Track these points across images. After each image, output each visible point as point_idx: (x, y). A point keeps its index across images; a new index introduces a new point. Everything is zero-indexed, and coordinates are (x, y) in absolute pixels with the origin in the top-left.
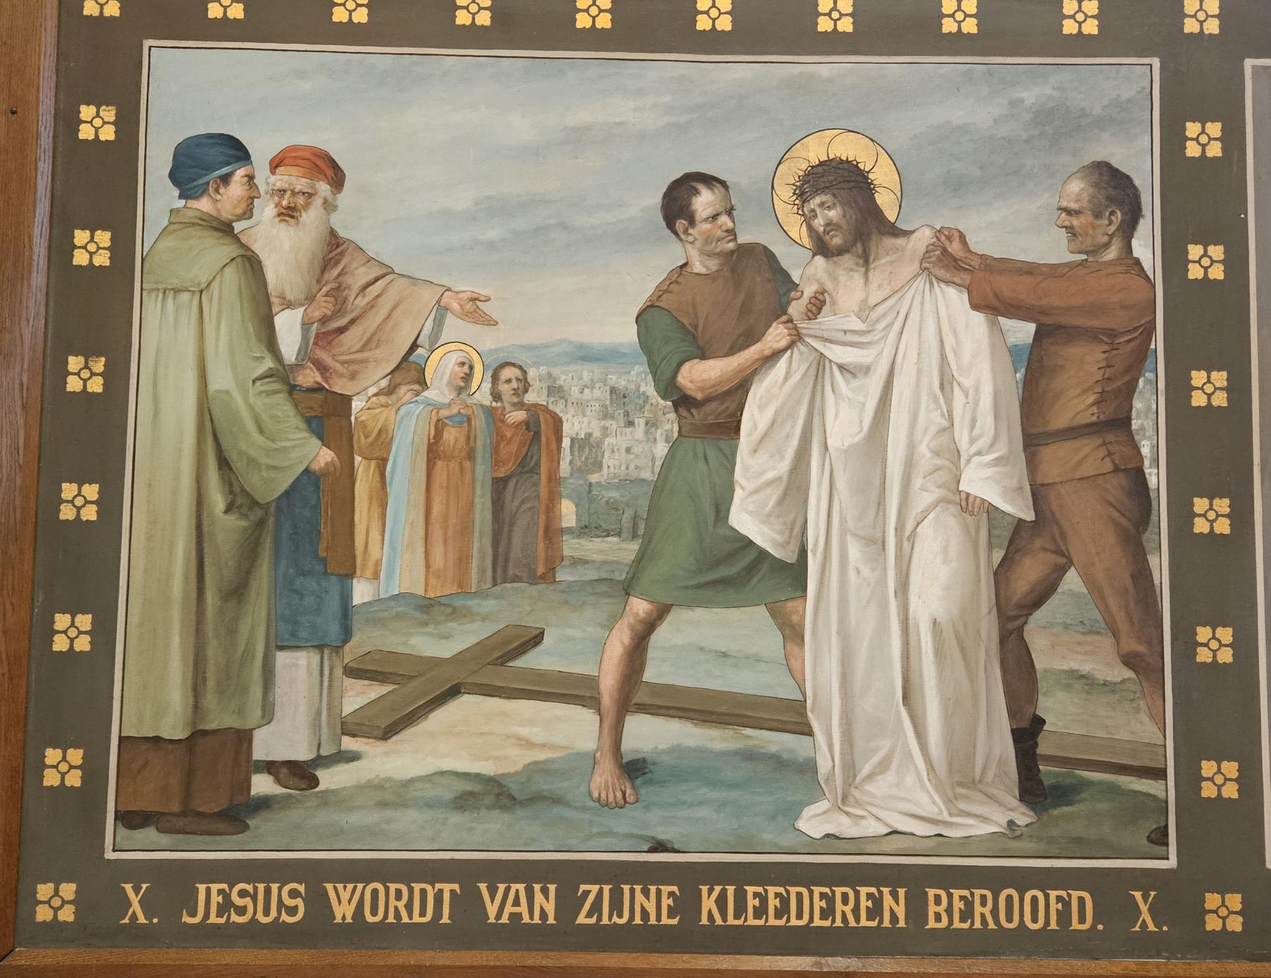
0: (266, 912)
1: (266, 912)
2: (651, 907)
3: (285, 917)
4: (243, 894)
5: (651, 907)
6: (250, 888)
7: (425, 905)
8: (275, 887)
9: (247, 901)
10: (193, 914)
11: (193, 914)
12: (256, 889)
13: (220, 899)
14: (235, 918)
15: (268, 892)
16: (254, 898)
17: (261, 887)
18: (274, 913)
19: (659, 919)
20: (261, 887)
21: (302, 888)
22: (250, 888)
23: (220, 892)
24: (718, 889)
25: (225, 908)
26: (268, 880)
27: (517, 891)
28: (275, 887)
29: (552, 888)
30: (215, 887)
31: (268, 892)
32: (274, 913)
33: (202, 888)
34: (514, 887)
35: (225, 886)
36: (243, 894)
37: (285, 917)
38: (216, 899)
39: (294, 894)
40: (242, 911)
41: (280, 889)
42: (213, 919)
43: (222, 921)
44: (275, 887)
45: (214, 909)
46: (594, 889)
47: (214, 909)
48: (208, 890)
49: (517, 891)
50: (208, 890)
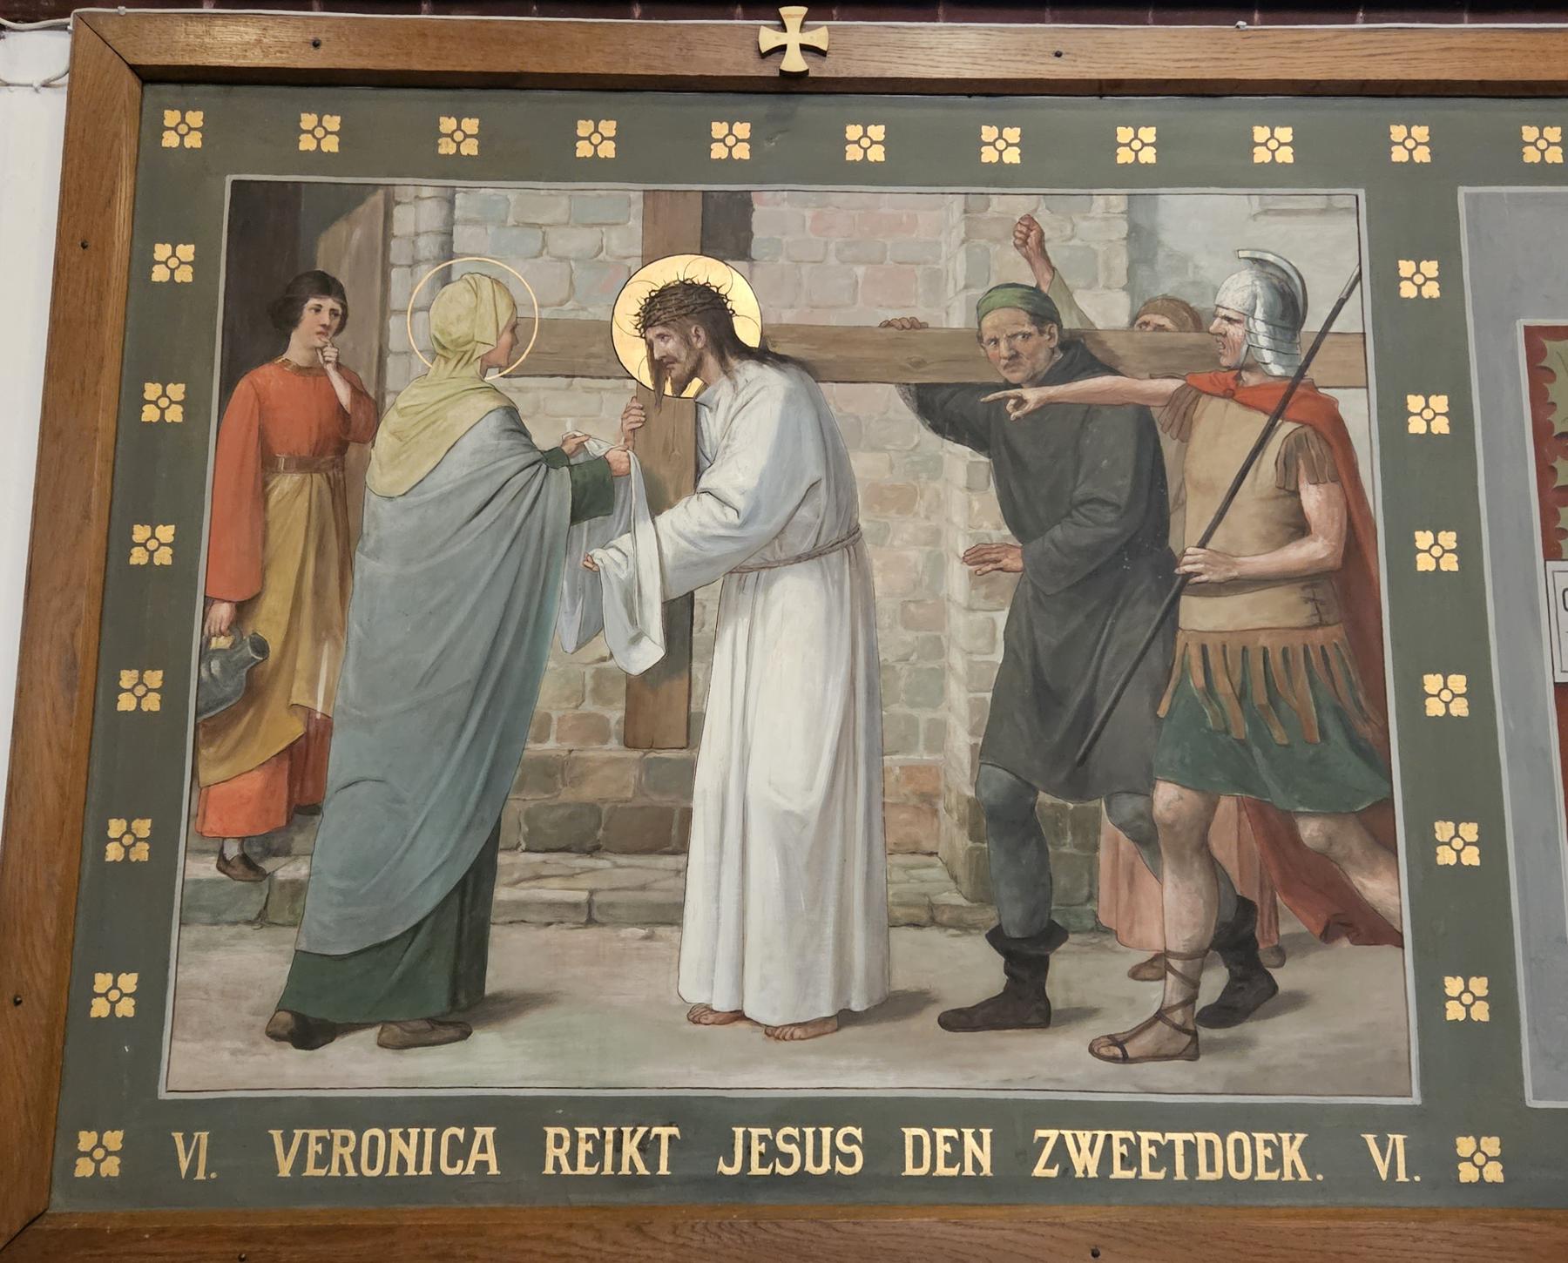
0: (818, 1161)
1: (818, 1161)
4: (788, 1139)
6: (795, 1132)
7: (836, 1152)
8: (826, 1132)
9: (793, 1149)
12: (803, 1135)
15: (818, 1136)
16: (802, 1146)
17: (809, 1131)
20: (809, 1131)
22: (795, 1132)
24: (642, 1130)
26: (818, 1123)
27: (484, 1138)
29: (986, 1132)
30: (755, 1132)
31: (818, 1136)
34: (480, 1131)
35: (767, 1131)
36: (788, 1139)
38: (757, 1148)
39: (849, 1139)
40: (787, 1160)
45: (755, 1158)
46: (1053, 1134)
47: (755, 1158)
48: (747, 1136)
49: (484, 1138)
50: (747, 1136)
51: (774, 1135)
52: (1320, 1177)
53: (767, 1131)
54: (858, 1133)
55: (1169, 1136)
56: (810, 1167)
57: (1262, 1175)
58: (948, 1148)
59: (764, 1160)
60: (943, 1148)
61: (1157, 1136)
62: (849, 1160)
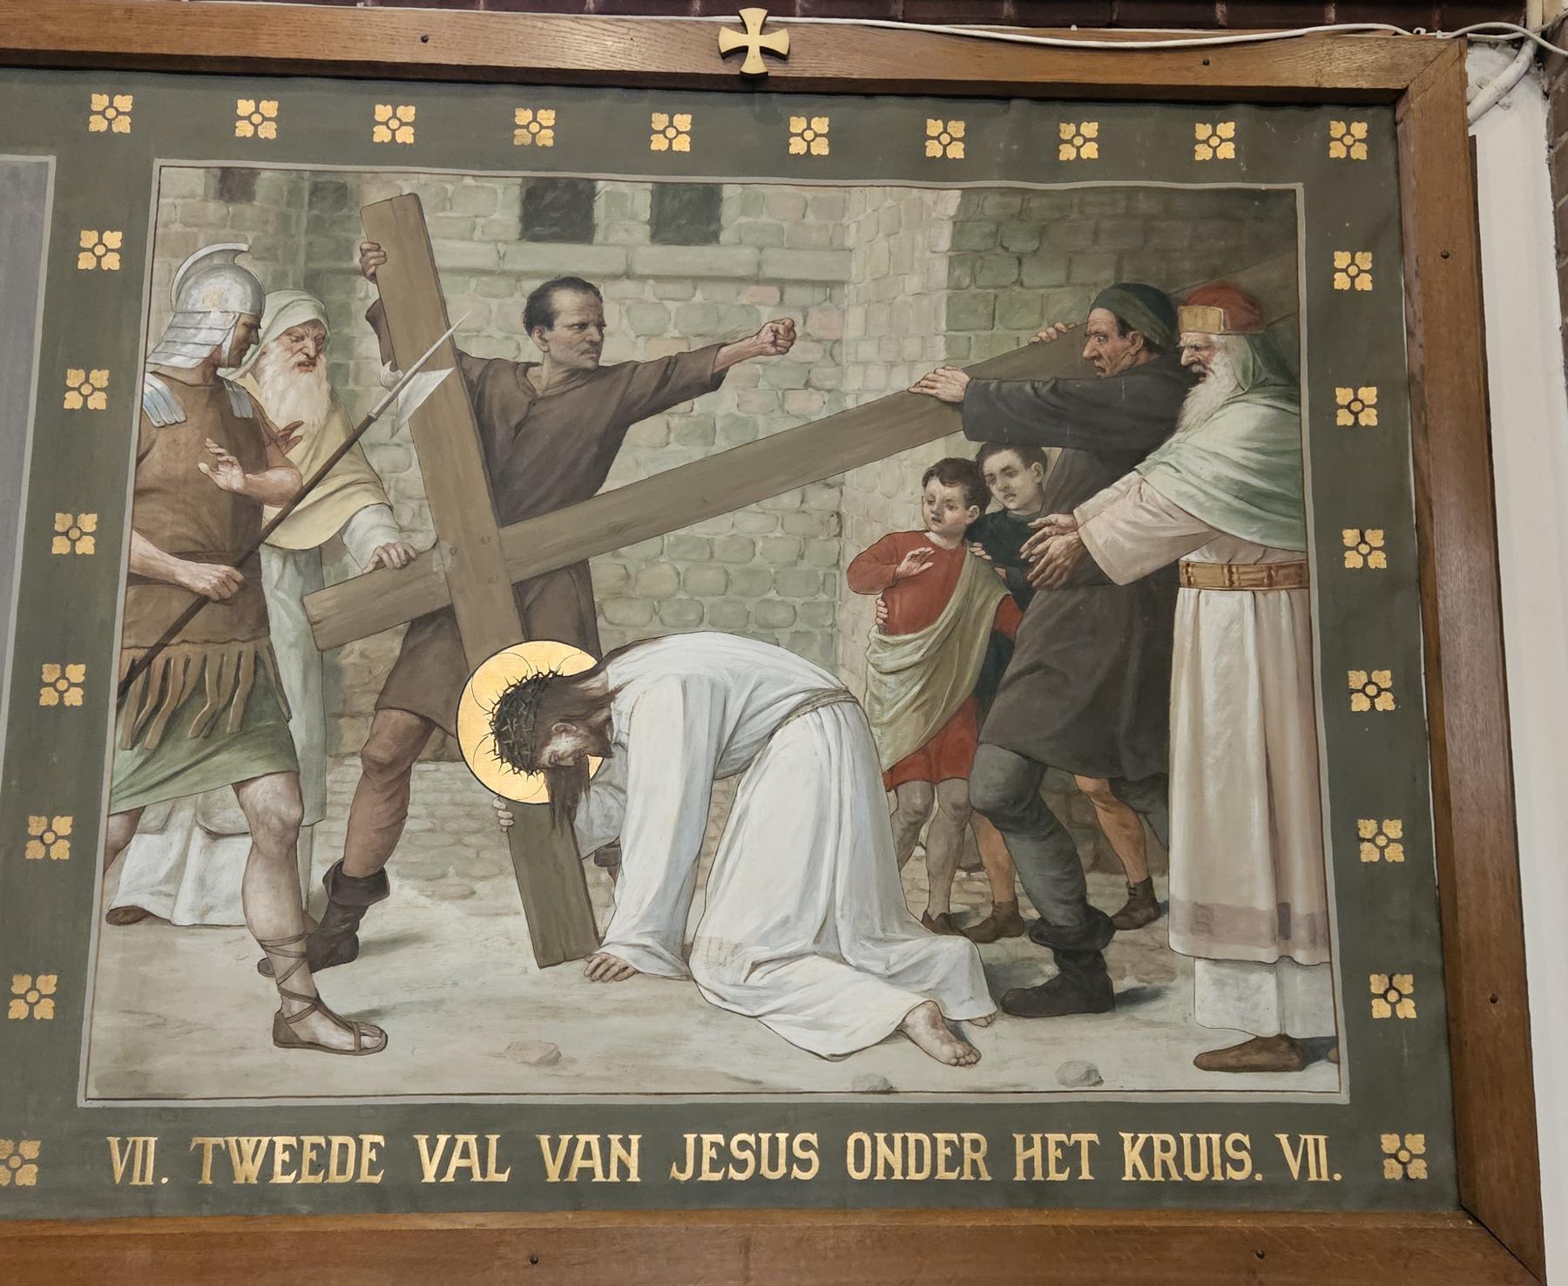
1: (773, 1166)
4: (743, 1145)
6: (751, 1139)
9: (748, 1155)
11: (682, 1170)
12: (758, 1141)
14: (734, 1174)
15: (774, 1142)
17: (765, 1137)
20: (765, 1137)
22: (751, 1139)
25: (723, 1157)
26: (773, 1128)
30: (707, 1139)
31: (774, 1142)
33: (690, 1138)
36: (743, 1145)
38: (709, 1153)
40: (741, 1165)
41: (790, 1141)
42: (707, 1175)
43: (718, 1176)
44: (782, 1137)
47: (706, 1166)
48: (699, 1143)
50: (699, 1143)
51: (728, 1140)
54: (813, 1138)
62: (805, 1165)
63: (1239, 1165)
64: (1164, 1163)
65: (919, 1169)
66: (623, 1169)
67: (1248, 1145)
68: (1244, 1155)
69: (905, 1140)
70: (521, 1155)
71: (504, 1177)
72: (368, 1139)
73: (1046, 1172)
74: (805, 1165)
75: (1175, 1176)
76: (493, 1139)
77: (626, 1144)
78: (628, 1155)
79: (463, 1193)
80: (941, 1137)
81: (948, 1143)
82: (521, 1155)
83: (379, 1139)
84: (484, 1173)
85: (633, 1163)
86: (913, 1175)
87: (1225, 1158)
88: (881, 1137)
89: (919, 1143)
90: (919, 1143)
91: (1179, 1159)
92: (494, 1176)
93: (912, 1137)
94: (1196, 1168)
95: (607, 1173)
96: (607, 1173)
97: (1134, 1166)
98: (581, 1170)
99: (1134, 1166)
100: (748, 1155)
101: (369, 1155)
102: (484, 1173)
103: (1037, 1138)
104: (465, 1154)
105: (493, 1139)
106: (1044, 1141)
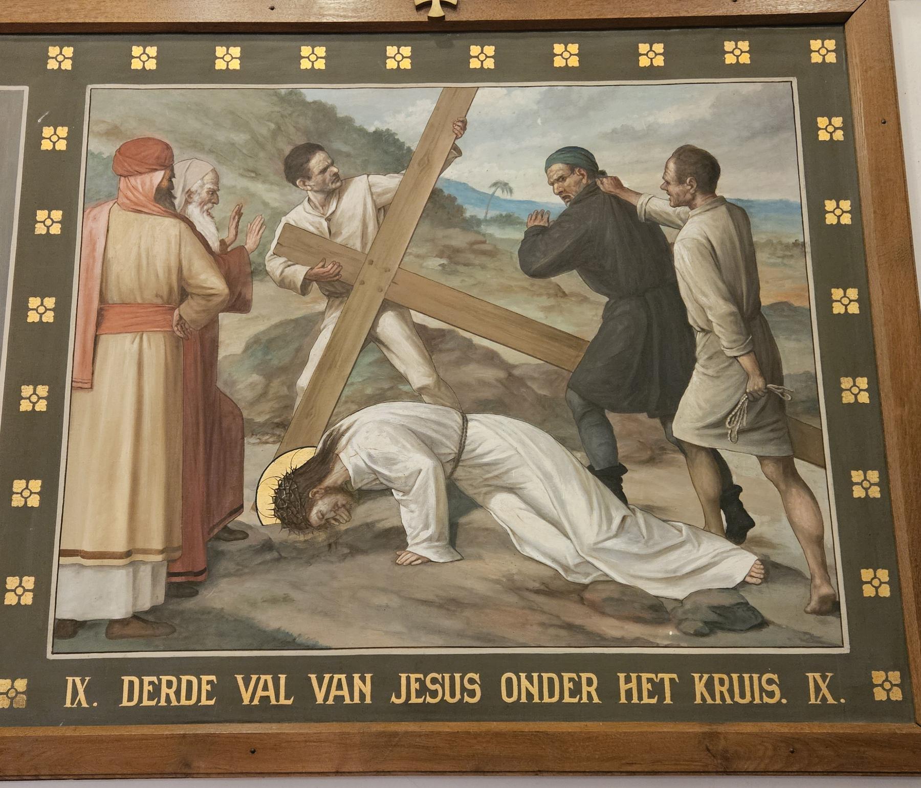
2: (535, 691)
3: (467, 699)
5: (535, 691)
6: (439, 677)
9: (438, 687)
10: (398, 696)
13: (417, 686)
14: (429, 700)
15: (452, 679)
18: (458, 696)
19: (640, 698)
21: (476, 677)
23: (417, 680)
26: (452, 672)
28: (457, 676)
31: (452, 679)
32: (458, 696)
35: (421, 676)
36: (434, 681)
37: (467, 699)
40: (434, 694)
43: (420, 701)
52: (842, 701)
53: (421, 676)
54: (476, 677)
55: (660, 676)
56: (447, 698)
57: (567, 699)
58: (571, 685)
59: (419, 694)
60: (568, 685)
61: (652, 676)
62: (472, 694)
63: (771, 694)
64: (721, 693)
65: (551, 695)
66: (362, 696)
67: (777, 680)
68: (774, 688)
69: (540, 679)
70: (300, 689)
71: (289, 702)
72: (205, 678)
73: (640, 698)
74: (472, 694)
75: (729, 701)
76: (283, 678)
77: (363, 679)
78: (363, 686)
79: (265, 711)
80: (566, 676)
81: (570, 680)
82: (300, 689)
83: (213, 678)
84: (277, 699)
85: (367, 690)
86: (546, 699)
87: (762, 689)
88: (523, 675)
89: (551, 680)
90: (551, 680)
91: (731, 691)
92: (283, 701)
93: (545, 676)
94: (743, 696)
95: (352, 698)
96: (352, 698)
97: (702, 694)
98: (336, 697)
99: (702, 694)
100: (438, 687)
101: (205, 688)
102: (277, 699)
103: (634, 676)
104: (265, 688)
105: (283, 678)
106: (639, 679)
